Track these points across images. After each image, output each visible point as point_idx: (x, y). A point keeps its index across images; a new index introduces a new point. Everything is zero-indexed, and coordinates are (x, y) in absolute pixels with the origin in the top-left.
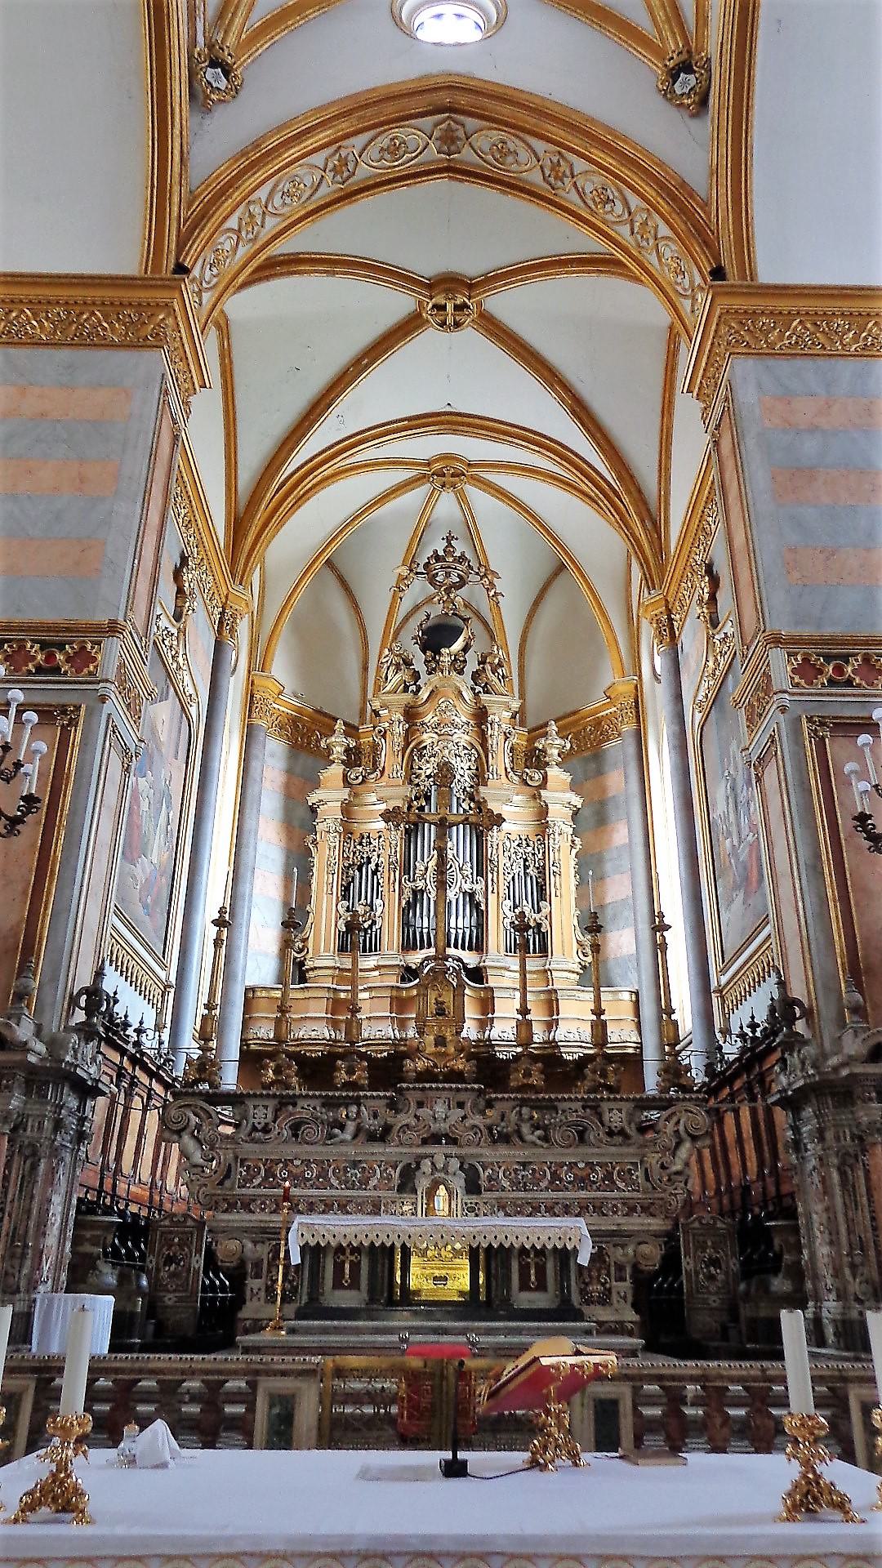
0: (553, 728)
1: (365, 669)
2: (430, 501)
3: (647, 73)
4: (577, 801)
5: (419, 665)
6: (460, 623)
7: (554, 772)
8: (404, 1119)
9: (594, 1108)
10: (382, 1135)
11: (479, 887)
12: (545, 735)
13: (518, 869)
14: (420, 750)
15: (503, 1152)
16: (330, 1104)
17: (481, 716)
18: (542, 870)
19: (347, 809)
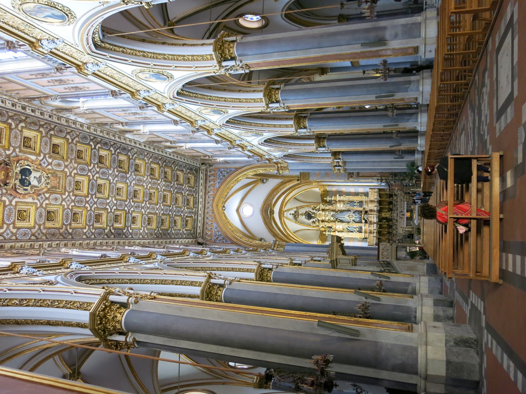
0: (325, 199)
1: (309, 229)
2: (287, 218)
3: (260, 186)
4: (338, 195)
5: (314, 220)
6: (307, 213)
7: (333, 199)
8: (395, 218)
9: (395, 200)
10: (397, 220)
11: (352, 211)
12: (326, 200)
13: (349, 205)
14: (329, 220)
15: (399, 209)
16: (394, 225)
17: (323, 210)
18: (349, 202)
19: (339, 232)
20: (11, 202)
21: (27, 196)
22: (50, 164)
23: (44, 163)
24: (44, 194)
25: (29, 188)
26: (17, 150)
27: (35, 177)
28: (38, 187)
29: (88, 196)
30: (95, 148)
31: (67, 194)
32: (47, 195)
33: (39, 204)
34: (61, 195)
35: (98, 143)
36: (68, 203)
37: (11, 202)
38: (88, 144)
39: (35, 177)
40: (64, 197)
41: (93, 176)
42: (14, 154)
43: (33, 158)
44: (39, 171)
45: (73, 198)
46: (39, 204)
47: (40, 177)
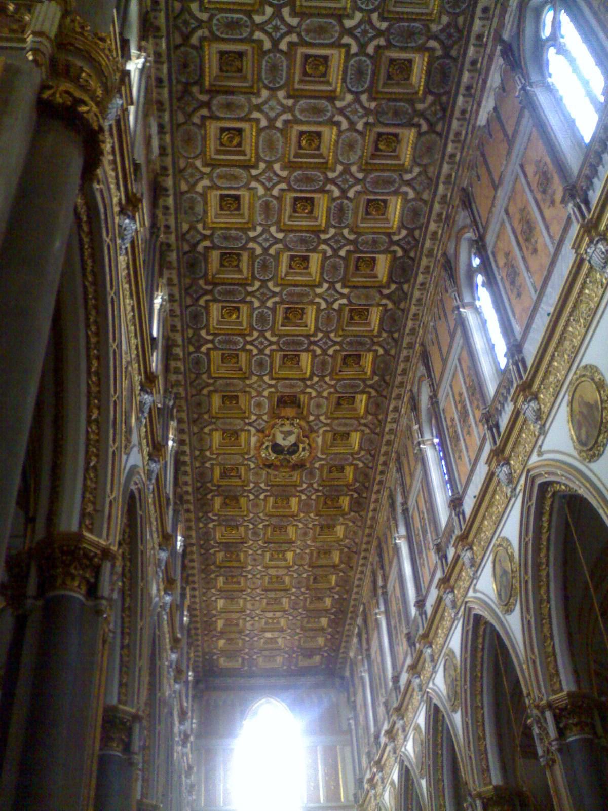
20: (321, 459)
21: (314, 445)
22: (259, 416)
23: (259, 424)
24: (308, 422)
25: (301, 446)
26: (246, 457)
27: (284, 440)
28: (299, 434)
29: (314, 351)
30: (212, 341)
31: (308, 390)
32: (311, 418)
33: (325, 429)
34: (311, 398)
35: (200, 336)
36: (325, 386)
37: (321, 459)
38: (207, 354)
39: (284, 440)
40: (314, 394)
41: (271, 343)
42: (253, 459)
43: (253, 440)
44: (274, 435)
45: (316, 379)
46: (325, 429)
47: (282, 432)
